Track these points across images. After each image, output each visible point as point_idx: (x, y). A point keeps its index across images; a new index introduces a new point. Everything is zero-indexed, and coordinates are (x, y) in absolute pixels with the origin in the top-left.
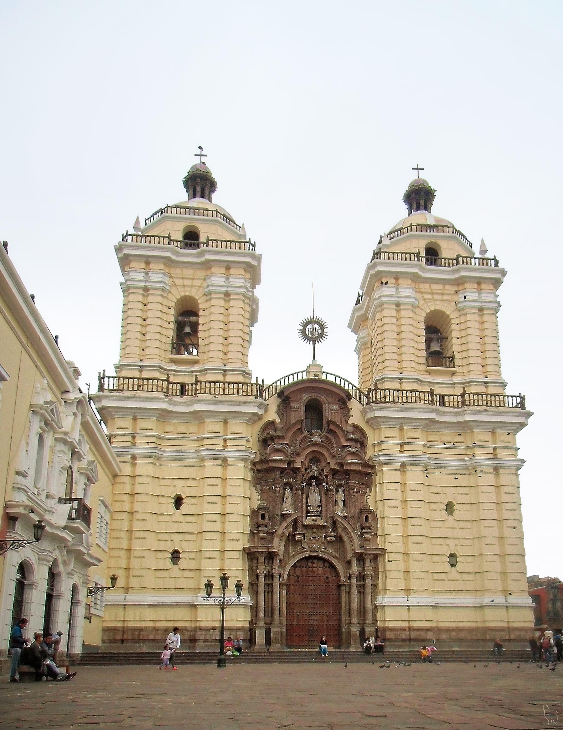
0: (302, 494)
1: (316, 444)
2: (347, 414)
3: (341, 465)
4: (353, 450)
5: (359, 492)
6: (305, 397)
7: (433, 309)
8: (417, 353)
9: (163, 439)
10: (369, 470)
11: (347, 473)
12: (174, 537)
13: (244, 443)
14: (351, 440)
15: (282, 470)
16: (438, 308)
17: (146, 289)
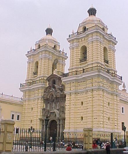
0: (51, 104)
1: (51, 92)
2: (61, 82)
3: (56, 96)
4: (58, 91)
5: (62, 102)
6: (52, 79)
7: (82, 46)
8: (77, 60)
9: (30, 95)
10: (64, 96)
11: (59, 97)
12: (32, 117)
13: (41, 94)
14: (58, 89)
15: (47, 99)
16: (83, 45)
17: (30, 62)
